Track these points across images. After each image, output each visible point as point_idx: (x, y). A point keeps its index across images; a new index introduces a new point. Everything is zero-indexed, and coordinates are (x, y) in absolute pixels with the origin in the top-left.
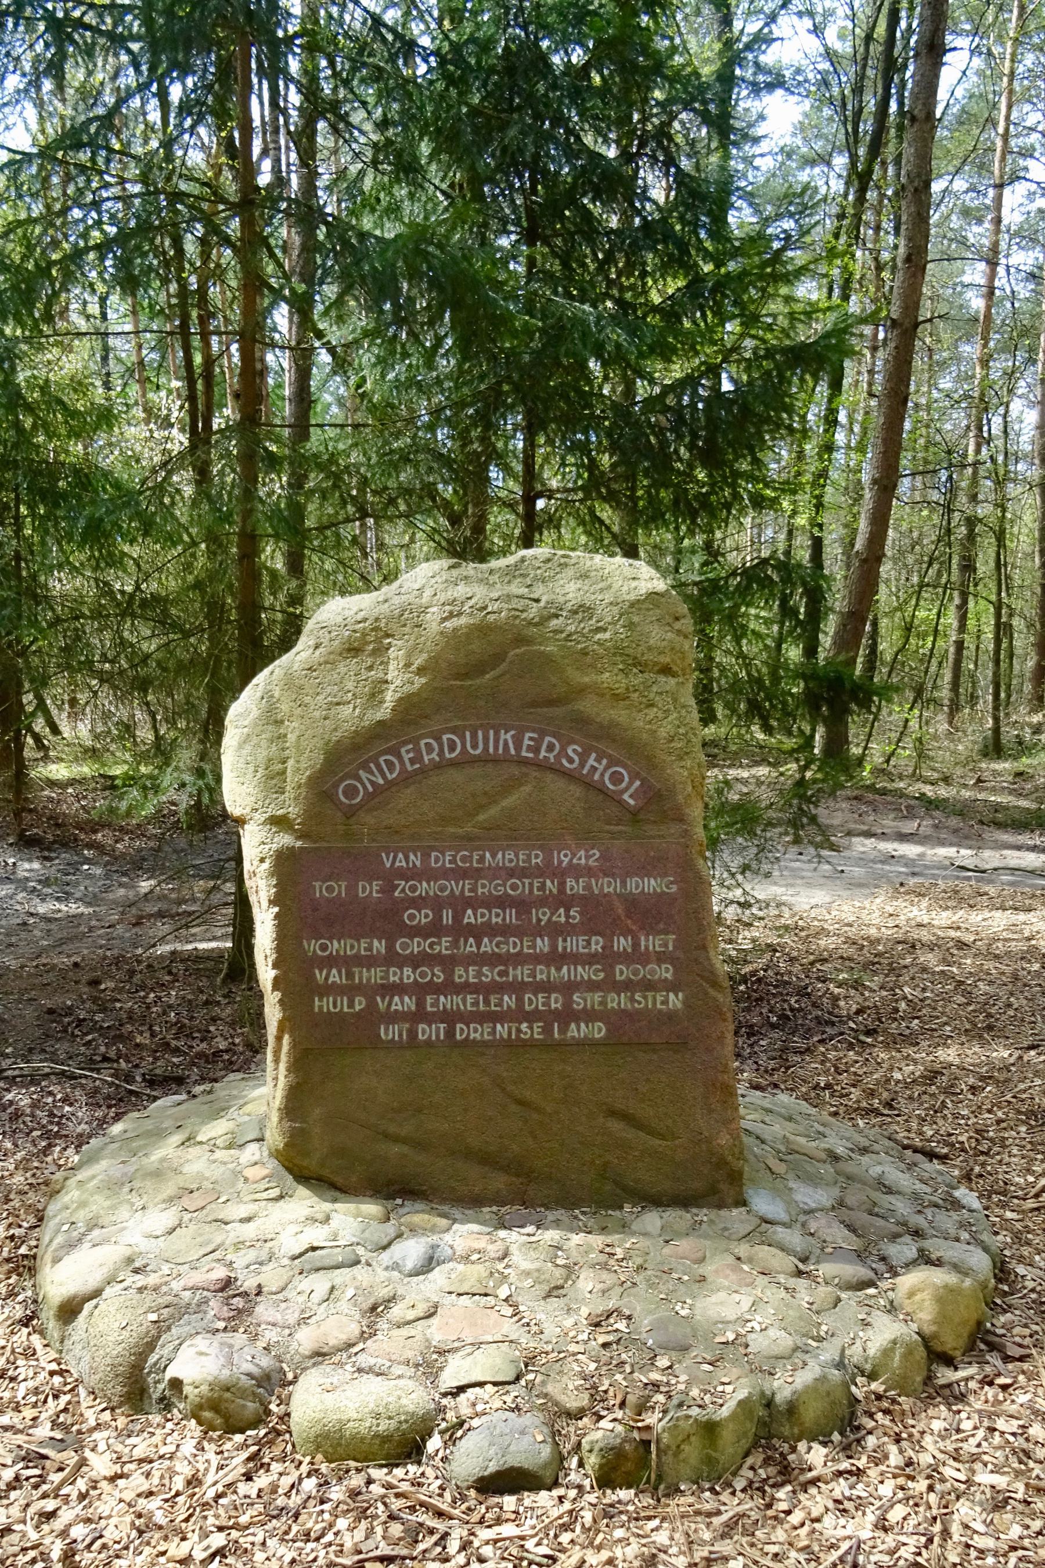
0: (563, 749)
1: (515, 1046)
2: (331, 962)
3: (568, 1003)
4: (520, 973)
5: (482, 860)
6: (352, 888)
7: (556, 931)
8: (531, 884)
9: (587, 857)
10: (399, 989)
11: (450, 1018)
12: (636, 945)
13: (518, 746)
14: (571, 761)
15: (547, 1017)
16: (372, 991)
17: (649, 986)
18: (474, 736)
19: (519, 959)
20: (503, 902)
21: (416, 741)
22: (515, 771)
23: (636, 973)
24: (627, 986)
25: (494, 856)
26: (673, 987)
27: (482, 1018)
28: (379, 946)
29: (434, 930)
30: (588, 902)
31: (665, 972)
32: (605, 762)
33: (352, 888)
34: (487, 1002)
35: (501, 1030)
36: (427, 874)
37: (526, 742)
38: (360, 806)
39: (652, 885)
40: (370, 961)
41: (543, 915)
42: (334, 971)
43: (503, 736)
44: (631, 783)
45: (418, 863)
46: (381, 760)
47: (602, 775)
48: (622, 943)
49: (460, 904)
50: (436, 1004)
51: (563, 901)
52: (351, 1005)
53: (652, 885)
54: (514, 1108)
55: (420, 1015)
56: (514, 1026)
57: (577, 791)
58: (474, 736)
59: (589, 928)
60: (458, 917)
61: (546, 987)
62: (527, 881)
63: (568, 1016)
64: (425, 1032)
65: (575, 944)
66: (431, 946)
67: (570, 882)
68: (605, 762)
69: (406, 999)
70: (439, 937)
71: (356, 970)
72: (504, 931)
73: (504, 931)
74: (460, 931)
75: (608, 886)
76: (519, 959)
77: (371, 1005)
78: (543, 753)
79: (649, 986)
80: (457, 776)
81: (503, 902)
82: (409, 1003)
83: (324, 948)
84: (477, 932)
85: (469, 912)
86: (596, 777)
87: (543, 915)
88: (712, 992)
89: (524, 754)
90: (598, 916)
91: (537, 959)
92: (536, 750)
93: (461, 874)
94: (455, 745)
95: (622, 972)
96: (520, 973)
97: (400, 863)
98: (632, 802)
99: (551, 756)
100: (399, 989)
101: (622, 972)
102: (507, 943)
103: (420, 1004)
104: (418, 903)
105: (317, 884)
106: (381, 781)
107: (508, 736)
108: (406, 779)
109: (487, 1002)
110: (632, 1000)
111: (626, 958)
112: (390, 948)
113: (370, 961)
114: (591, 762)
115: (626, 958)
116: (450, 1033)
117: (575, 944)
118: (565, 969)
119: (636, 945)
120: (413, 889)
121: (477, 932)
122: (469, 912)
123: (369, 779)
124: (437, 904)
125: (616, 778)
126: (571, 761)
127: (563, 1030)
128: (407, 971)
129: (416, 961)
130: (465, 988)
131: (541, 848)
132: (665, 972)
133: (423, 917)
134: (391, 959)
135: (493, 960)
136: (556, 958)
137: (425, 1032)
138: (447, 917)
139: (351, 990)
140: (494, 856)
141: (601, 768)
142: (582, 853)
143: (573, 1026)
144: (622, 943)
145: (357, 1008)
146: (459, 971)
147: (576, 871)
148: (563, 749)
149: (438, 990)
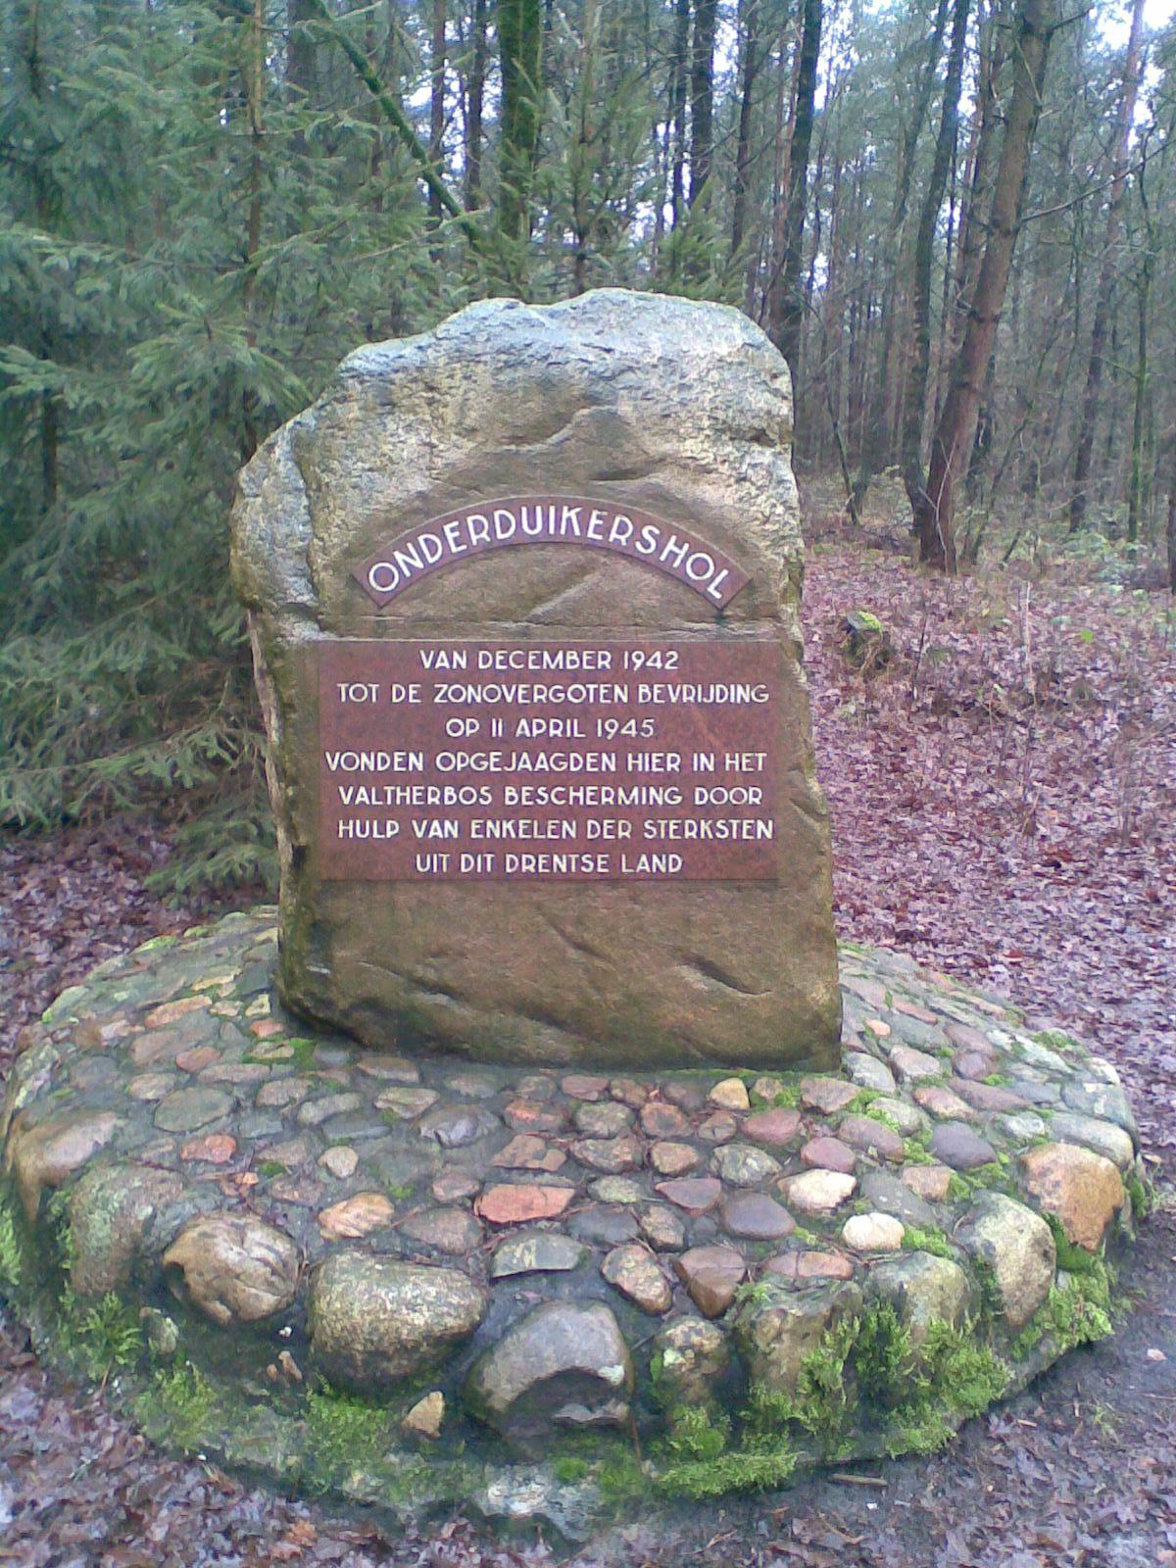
0: (637, 531)
1: (580, 882)
2: (360, 778)
3: (638, 831)
4: (583, 795)
5: (539, 660)
6: (385, 693)
7: (622, 746)
8: (597, 691)
9: (664, 660)
10: (441, 813)
11: (501, 847)
12: (720, 764)
13: (584, 527)
14: (647, 546)
15: (613, 848)
16: (405, 814)
17: (734, 812)
18: (532, 514)
19: (582, 779)
20: (564, 711)
21: (461, 518)
22: (580, 557)
23: (719, 796)
24: (708, 812)
25: (553, 658)
26: (762, 812)
27: (534, 847)
28: (416, 762)
29: (482, 743)
30: (668, 715)
31: (752, 796)
32: (686, 546)
33: (385, 693)
34: (543, 830)
35: (560, 863)
36: (472, 676)
37: (594, 521)
38: (395, 593)
39: (741, 693)
40: (407, 779)
41: (610, 728)
42: (362, 790)
43: (565, 514)
44: (717, 573)
45: (463, 664)
46: (421, 539)
47: (684, 562)
48: (705, 762)
49: (511, 713)
50: (482, 830)
51: (631, 710)
52: (382, 830)
53: (741, 693)
54: (572, 953)
55: (464, 844)
56: (574, 857)
57: (651, 579)
58: (532, 514)
59: (662, 742)
60: (510, 727)
61: (615, 811)
62: (592, 687)
63: (638, 846)
64: (467, 863)
65: (645, 763)
66: (477, 762)
67: (643, 689)
68: (686, 546)
69: (447, 824)
70: (488, 753)
71: (389, 789)
72: (566, 745)
73: (566, 745)
74: (510, 744)
75: (686, 694)
76: (582, 779)
77: (406, 832)
78: (613, 535)
79: (734, 812)
80: (511, 560)
81: (564, 711)
82: (451, 829)
83: (350, 762)
84: (533, 746)
85: (523, 722)
86: (677, 564)
87: (610, 728)
88: (810, 821)
89: (591, 534)
90: (678, 728)
91: (601, 778)
92: (605, 531)
93: (511, 678)
94: (505, 523)
95: (702, 796)
96: (583, 795)
97: (443, 662)
98: (718, 595)
99: (623, 538)
100: (441, 813)
101: (702, 796)
102: (568, 760)
103: (464, 830)
104: (466, 710)
105: (343, 687)
106: (419, 564)
107: (573, 514)
108: (449, 564)
109: (543, 830)
110: (713, 828)
111: (705, 779)
112: (429, 763)
113: (407, 779)
114: (671, 546)
115: (705, 779)
116: (499, 864)
117: (645, 763)
118: (635, 792)
119: (720, 764)
120: (457, 694)
121: (533, 746)
122: (523, 722)
123: (406, 561)
124: (484, 712)
125: (700, 567)
126: (647, 546)
127: (632, 865)
128: (449, 791)
129: (458, 780)
130: (515, 813)
131: (611, 648)
132: (752, 796)
133: (468, 728)
134: (431, 776)
135: (547, 779)
136: (625, 778)
137: (467, 863)
138: (498, 728)
139: (382, 814)
140: (553, 658)
141: (682, 553)
142: (658, 654)
143: (644, 858)
144: (705, 762)
145: (389, 834)
146: (510, 791)
147: (648, 675)
148: (637, 531)
149: (484, 813)
